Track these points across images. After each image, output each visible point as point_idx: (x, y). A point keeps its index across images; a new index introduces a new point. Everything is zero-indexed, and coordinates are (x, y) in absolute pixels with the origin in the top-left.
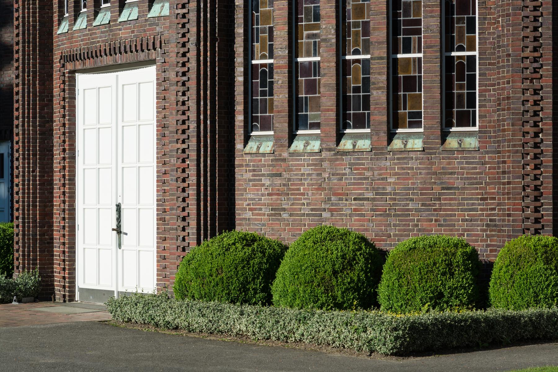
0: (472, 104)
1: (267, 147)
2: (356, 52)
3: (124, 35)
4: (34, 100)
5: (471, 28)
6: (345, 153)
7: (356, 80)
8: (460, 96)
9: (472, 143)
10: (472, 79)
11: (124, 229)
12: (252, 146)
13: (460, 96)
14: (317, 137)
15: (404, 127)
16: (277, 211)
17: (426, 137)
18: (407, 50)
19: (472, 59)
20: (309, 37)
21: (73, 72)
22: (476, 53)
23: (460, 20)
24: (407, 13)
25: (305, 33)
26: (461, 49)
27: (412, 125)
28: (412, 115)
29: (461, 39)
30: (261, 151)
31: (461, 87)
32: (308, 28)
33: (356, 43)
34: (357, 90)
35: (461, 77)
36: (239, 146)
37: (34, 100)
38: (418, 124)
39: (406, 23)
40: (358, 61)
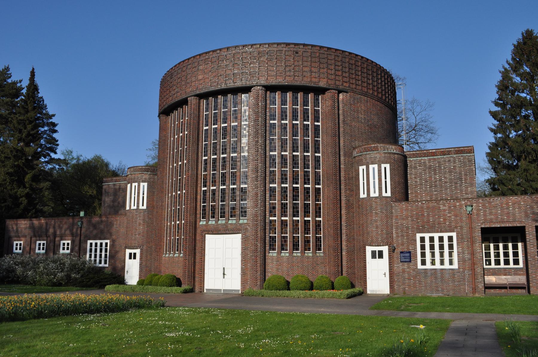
0: (321, 246)
1: (275, 255)
2: (296, 234)
3: (229, 227)
4: (192, 241)
5: (321, 230)
6: (295, 256)
7: (296, 240)
8: (318, 244)
9: (322, 255)
10: (321, 241)
11: (225, 273)
12: (271, 254)
13: (318, 244)
14: (287, 253)
15: (307, 251)
16: (278, 269)
17: (312, 253)
18: (307, 234)
19: (321, 237)
20: (285, 230)
21: (205, 234)
22: (322, 235)
23: (318, 228)
24: (307, 226)
25: (284, 229)
26: (318, 234)
27: (309, 250)
28: (308, 248)
29: (319, 232)
30: (274, 255)
31: (318, 243)
32: (284, 228)
33: (296, 232)
34: (296, 242)
35: (318, 241)
36: (267, 254)
37: (192, 241)
38: (310, 250)
39: (307, 228)
40: (296, 236)
